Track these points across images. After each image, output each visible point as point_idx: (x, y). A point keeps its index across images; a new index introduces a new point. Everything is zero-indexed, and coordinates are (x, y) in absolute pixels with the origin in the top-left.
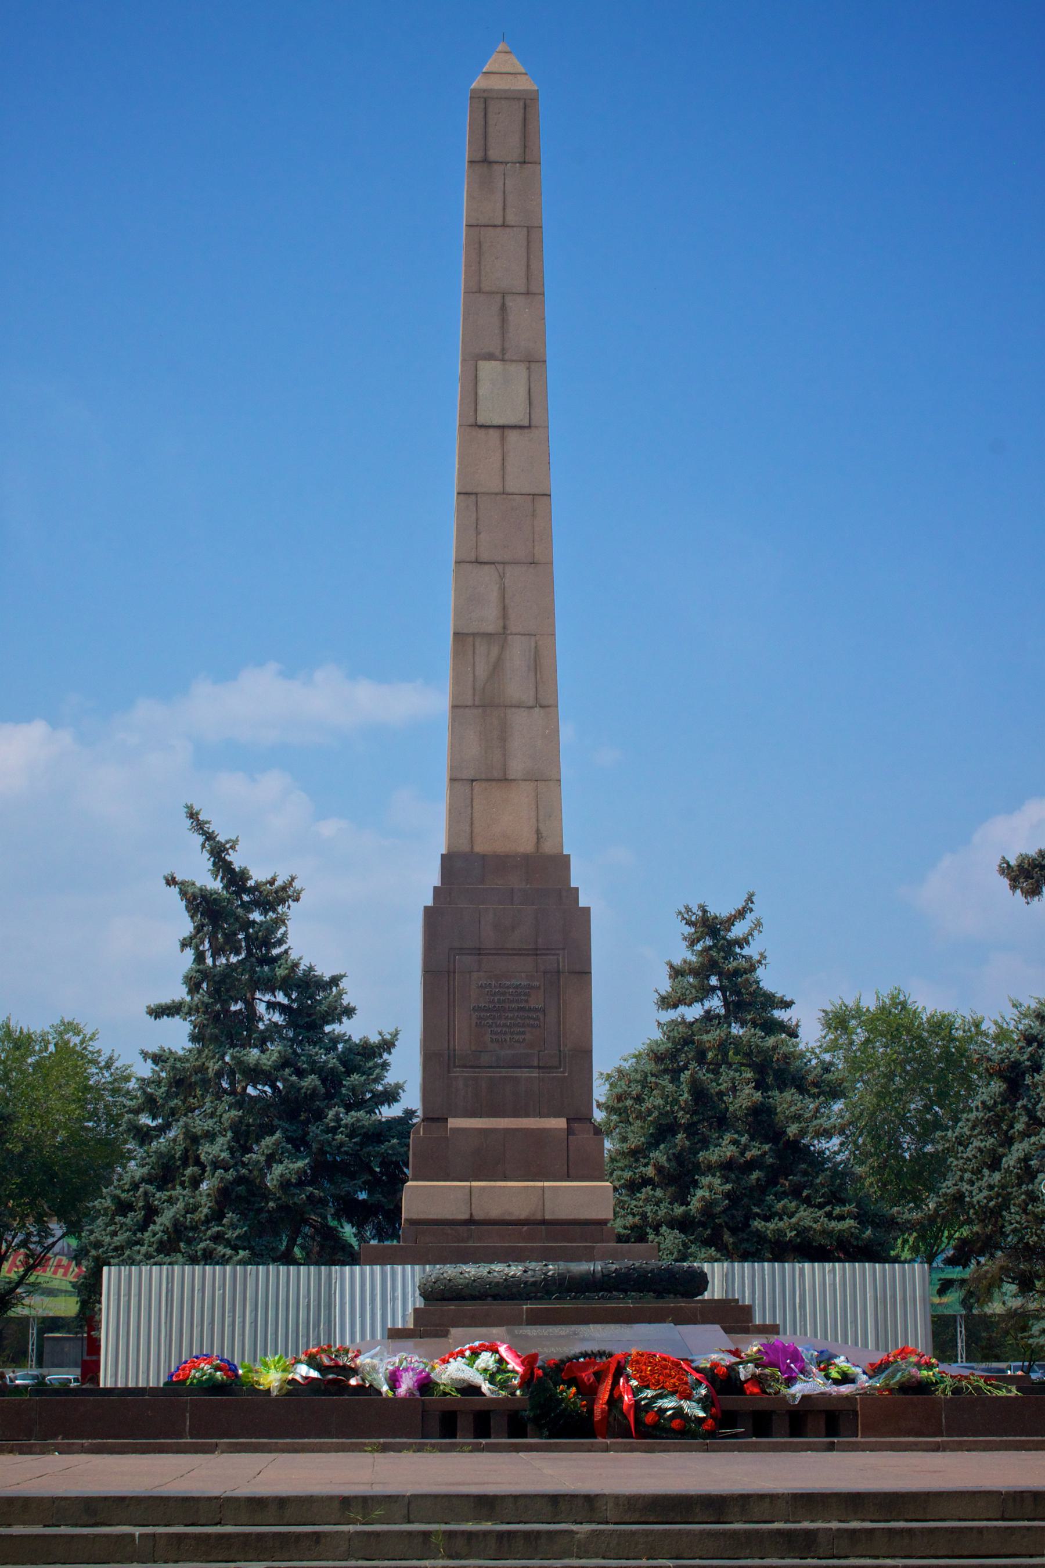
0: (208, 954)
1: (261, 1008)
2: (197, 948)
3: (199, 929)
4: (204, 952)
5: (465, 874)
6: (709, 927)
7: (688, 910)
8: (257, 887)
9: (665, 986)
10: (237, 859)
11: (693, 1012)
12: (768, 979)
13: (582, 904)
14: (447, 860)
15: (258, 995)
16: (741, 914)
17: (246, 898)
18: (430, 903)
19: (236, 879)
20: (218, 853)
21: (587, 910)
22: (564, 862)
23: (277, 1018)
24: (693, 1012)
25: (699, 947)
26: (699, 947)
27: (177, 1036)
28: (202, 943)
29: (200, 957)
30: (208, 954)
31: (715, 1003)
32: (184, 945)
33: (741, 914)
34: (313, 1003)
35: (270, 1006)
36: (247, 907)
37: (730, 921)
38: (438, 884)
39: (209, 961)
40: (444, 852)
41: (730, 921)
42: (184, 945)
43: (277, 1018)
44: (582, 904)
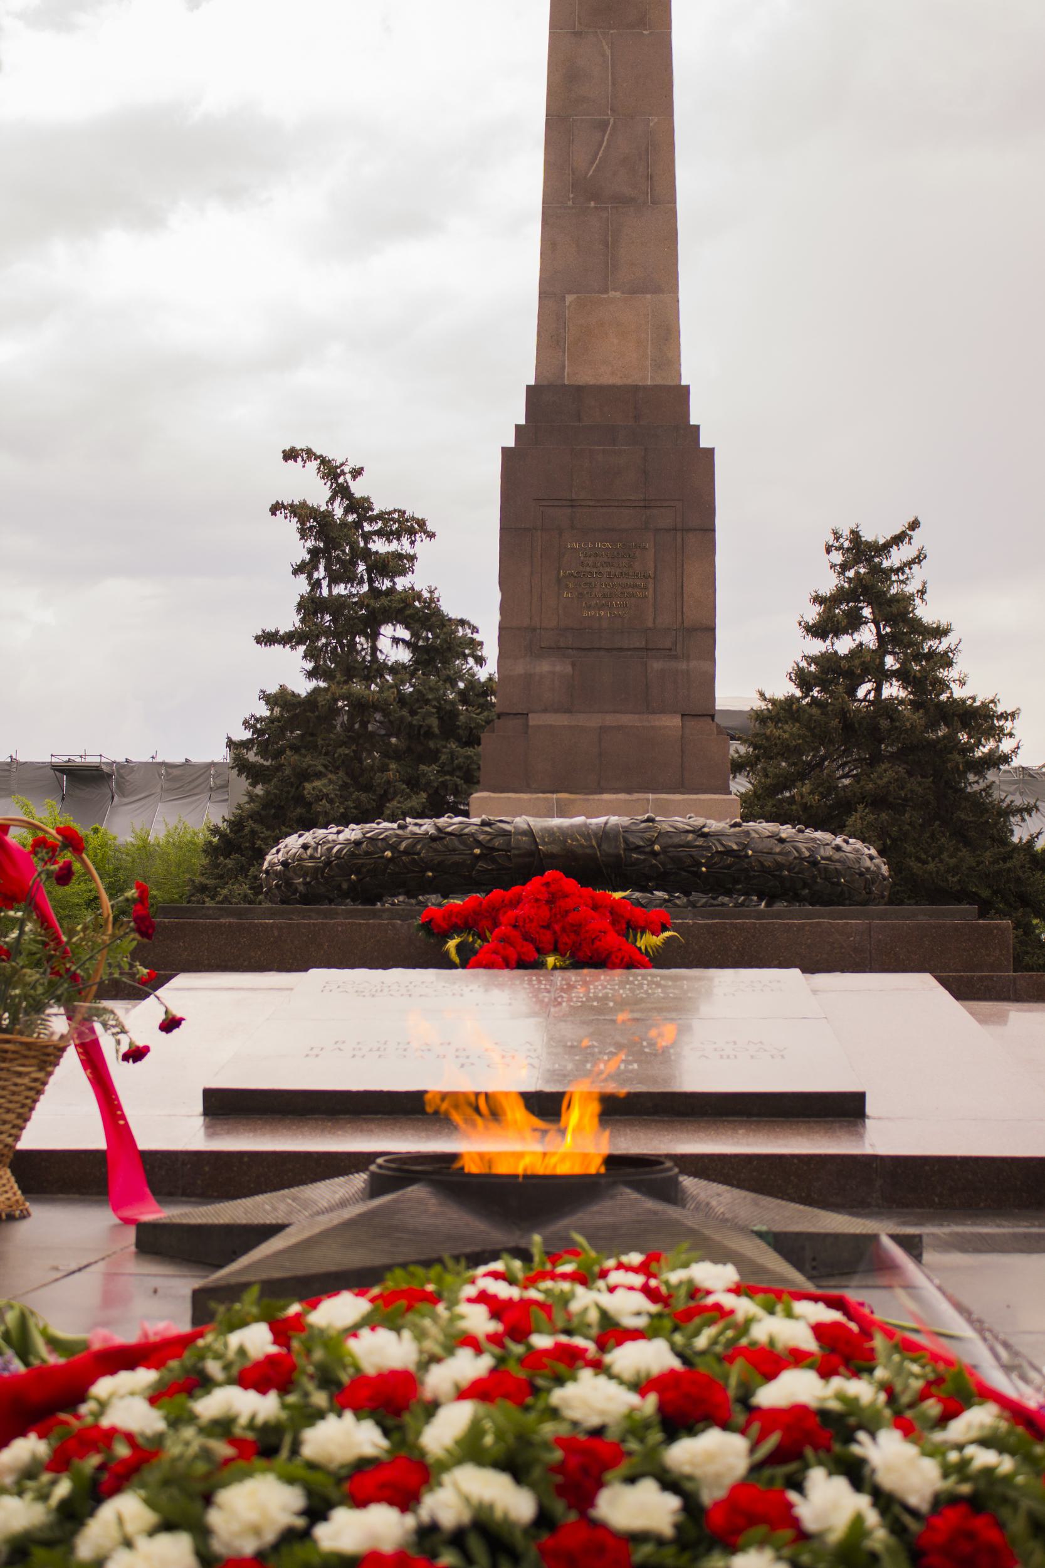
0: (325, 583)
1: (384, 643)
2: (310, 577)
3: (314, 552)
4: (318, 581)
5: (553, 408)
6: (860, 550)
7: (837, 536)
8: (381, 516)
9: (812, 614)
10: (358, 488)
11: (844, 645)
12: (926, 613)
13: (703, 445)
14: (532, 392)
15: (383, 630)
16: (898, 539)
17: (367, 527)
18: (511, 443)
19: (359, 506)
20: (330, 471)
21: (711, 451)
22: (682, 394)
23: (403, 655)
24: (844, 645)
25: (851, 574)
26: (851, 574)
27: (292, 671)
28: (317, 569)
29: (316, 585)
30: (325, 583)
31: (867, 636)
32: (298, 570)
33: (898, 539)
34: (440, 640)
35: (396, 641)
36: (367, 537)
37: (886, 548)
38: (523, 422)
39: (325, 592)
40: (532, 383)
41: (886, 548)
42: (297, 571)
43: (403, 655)
44: (703, 445)
